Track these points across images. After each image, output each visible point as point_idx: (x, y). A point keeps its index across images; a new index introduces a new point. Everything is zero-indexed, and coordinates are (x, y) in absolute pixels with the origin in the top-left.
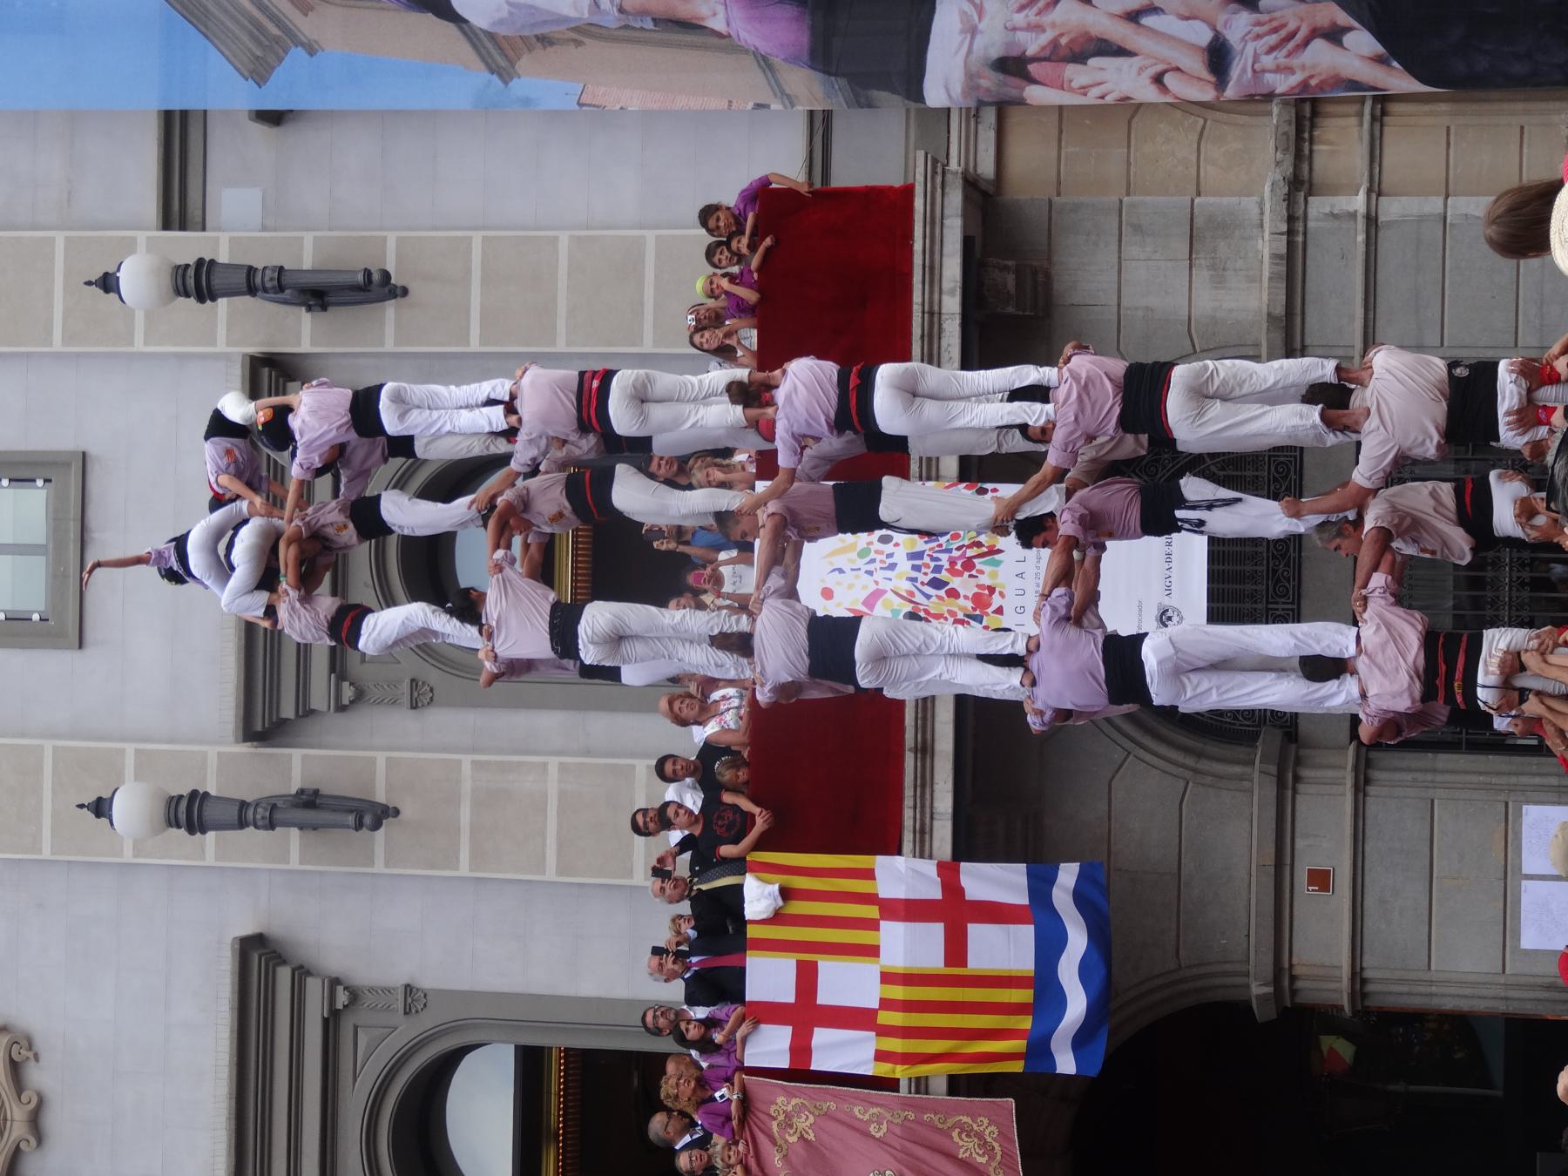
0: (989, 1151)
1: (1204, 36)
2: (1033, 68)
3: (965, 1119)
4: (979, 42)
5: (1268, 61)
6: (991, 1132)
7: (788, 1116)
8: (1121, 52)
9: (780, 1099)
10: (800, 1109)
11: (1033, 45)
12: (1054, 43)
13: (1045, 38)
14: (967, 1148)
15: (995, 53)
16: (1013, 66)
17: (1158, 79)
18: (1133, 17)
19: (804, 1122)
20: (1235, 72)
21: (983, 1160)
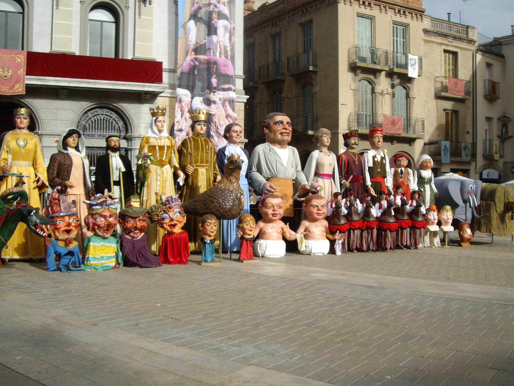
0: (16, 90)
1: (183, 129)
2: (180, 104)
3: (22, 86)
4: (184, 96)
5: (180, 137)
6: (20, 90)
7: (20, 58)
8: (182, 116)
9: (23, 57)
10: (22, 60)
11: (183, 104)
12: (183, 107)
13: (184, 106)
14: (17, 86)
15: (182, 99)
16: (180, 101)
17: (178, 122)
18: (186, 119)
19: (19, 60)
20: (178, 133)
21: (15, 88)
